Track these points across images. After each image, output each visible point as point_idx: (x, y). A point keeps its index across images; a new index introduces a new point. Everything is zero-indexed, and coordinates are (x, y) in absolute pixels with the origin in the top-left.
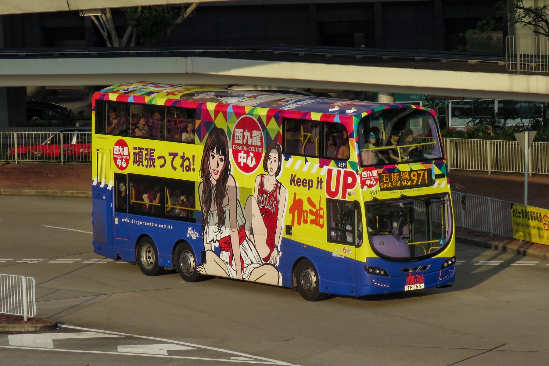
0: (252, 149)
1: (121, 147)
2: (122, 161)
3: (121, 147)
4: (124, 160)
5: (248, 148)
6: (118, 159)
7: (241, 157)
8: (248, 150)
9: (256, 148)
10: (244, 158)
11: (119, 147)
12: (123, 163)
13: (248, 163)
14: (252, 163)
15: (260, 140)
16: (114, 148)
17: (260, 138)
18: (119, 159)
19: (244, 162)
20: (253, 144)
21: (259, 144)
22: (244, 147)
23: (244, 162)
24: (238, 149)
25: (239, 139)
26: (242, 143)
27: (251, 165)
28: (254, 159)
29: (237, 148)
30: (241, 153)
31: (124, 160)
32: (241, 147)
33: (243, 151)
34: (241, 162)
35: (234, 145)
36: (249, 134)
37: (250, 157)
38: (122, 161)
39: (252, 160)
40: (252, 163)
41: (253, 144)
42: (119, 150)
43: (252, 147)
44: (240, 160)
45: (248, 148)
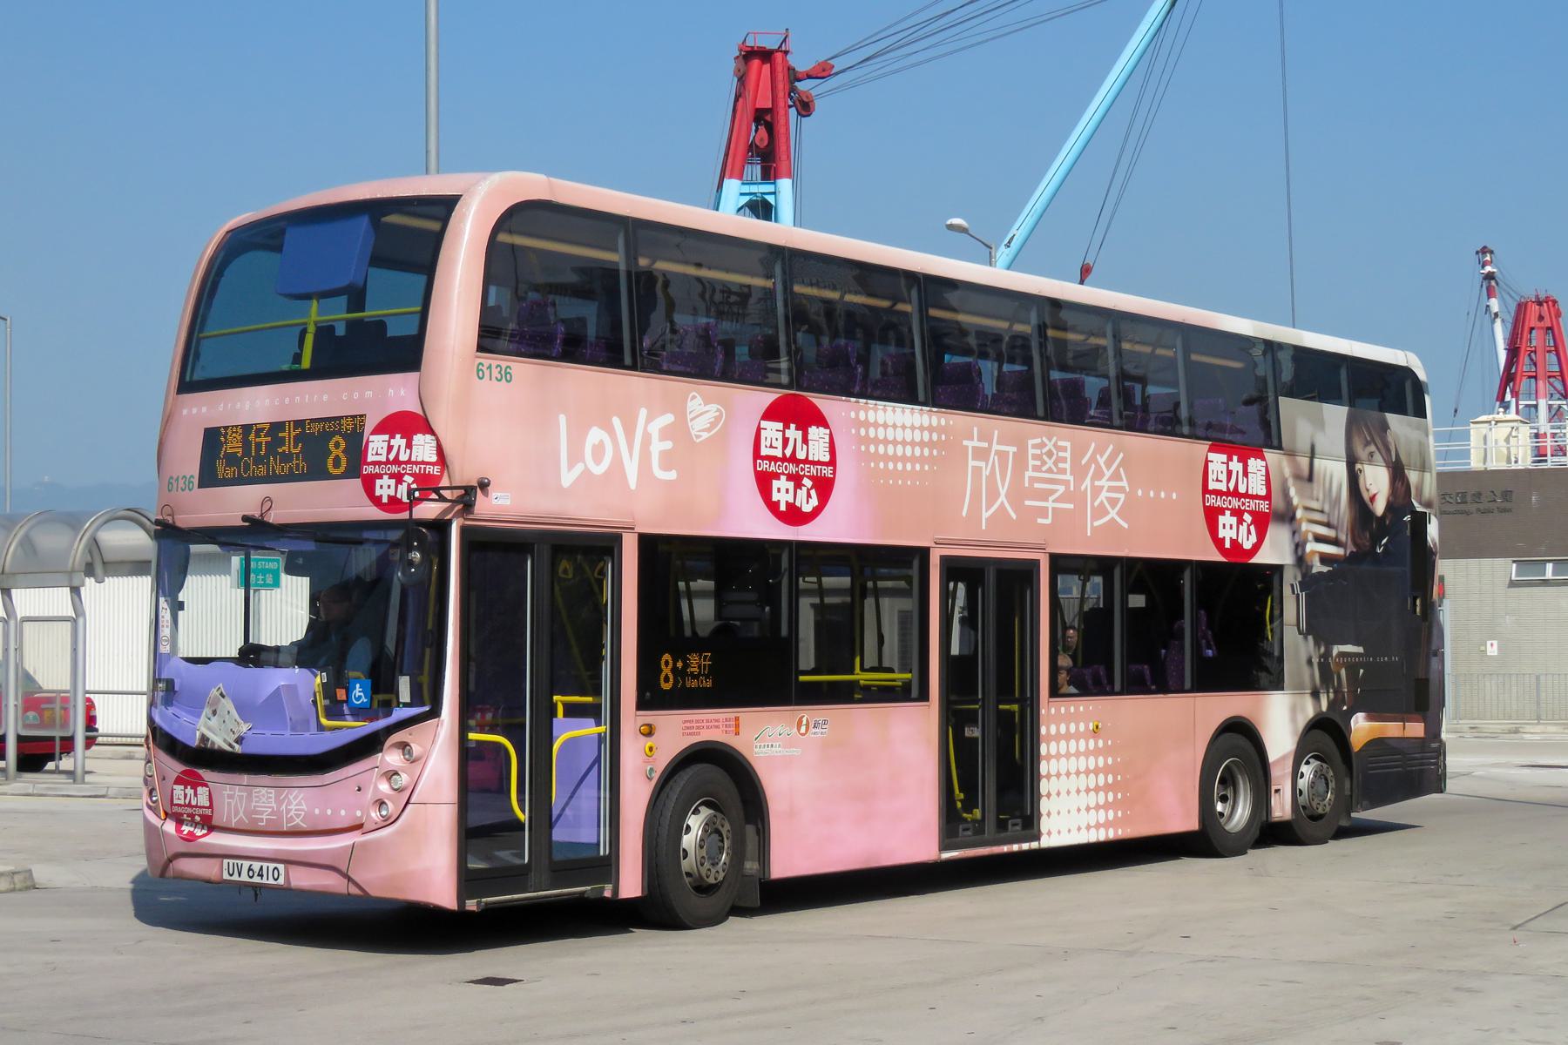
0: (806, 470)
1: (793, 426)
2: (798, 485)
3: (793, 426)
4: (807, 482)
6: (777, 476)
7: (779, 490)
8: (797, 472)
9: (819, 467)
10: (787, 491)
11: (787, 427)
12: (802, 493)
13: (798, 504)
14: (808, 503)
15: (828, 450)
16: (759, 430)
17: (828, 445)
18: (783, 478)
19: (787, 502)
21: (827, 458)
23: (787, 502)
24: (771, 469)
25: (773, 445)
26: (780, 455)
27: (807, 508)
28: (813, 492)
29: (767, 466)
30: (779, 479)
31: (807, 482)
32: (779, 465)
33: (783, 474)
34: (779, 501)
35: (758, 461)
37: (803, 488)
38: (798, 485)
39: (809, 496)
40: (808, 503)
41: (810, 458)
42: (786, 441)
43: (807, 466)
44: (775, 497)
45: (797, 466)
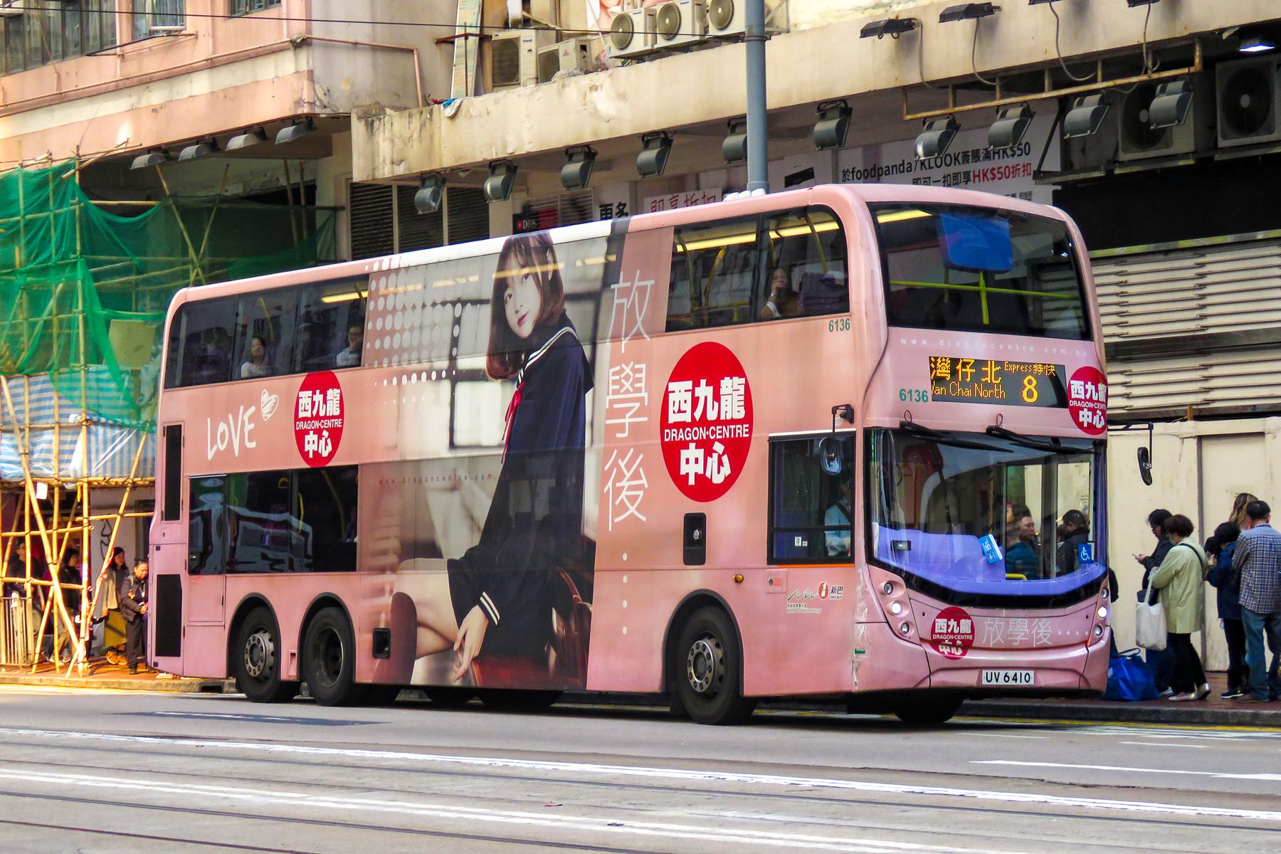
0: (718, 432)
2: (709, 452)
5: (708, 430)
8: (708, 436)
9: (732, 427)
10: (697, 461)
14: (719, 472)
19: (696, 474)
20: (723, 418)
22: (696, 429)
23: (696, 474)
24: (680, 437)
25: (682, 409)
27: (718, 479)
28: (725, 459)
29: (675, 435)
32: (688, 432)
34: (687, 474)
35: (666, 431)
36: (709, 391)
38: (709, 452)
39: (720, 463)
40: (719, 472)
44: (684, 469)
45: (708, 430)
